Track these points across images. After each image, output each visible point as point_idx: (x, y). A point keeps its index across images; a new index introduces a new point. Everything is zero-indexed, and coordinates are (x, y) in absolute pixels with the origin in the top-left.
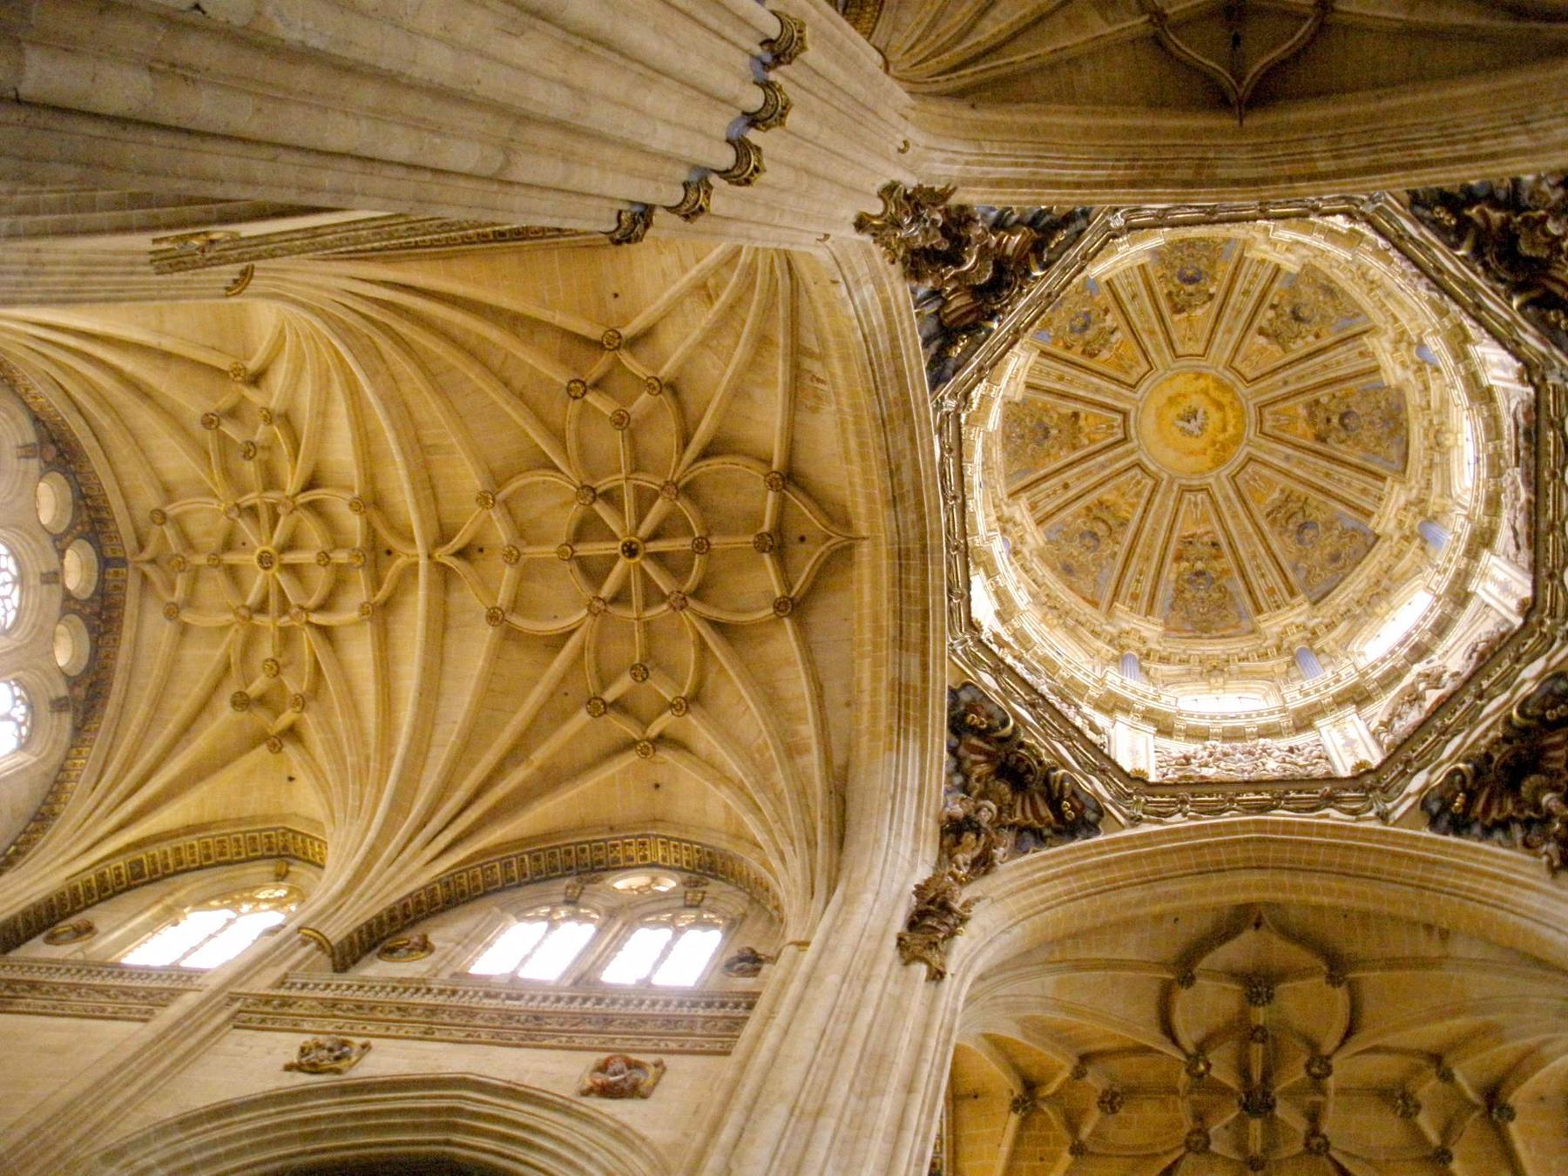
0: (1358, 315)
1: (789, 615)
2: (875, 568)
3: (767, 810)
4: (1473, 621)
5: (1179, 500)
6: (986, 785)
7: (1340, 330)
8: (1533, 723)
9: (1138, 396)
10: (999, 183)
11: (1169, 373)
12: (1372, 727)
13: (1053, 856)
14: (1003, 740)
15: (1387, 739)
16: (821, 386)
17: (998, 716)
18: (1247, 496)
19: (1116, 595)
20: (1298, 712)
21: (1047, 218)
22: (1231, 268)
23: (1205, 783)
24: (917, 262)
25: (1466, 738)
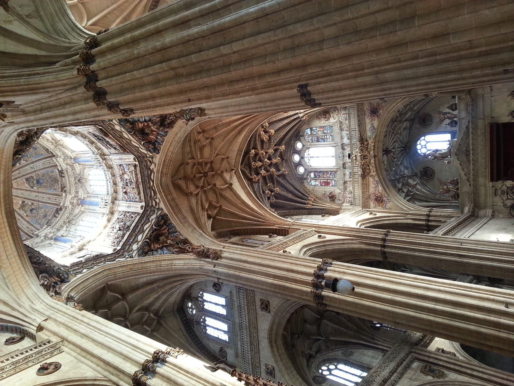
0: (40, 224)
10: (176, 134)
14: (32, 137)
22: (44, 191)
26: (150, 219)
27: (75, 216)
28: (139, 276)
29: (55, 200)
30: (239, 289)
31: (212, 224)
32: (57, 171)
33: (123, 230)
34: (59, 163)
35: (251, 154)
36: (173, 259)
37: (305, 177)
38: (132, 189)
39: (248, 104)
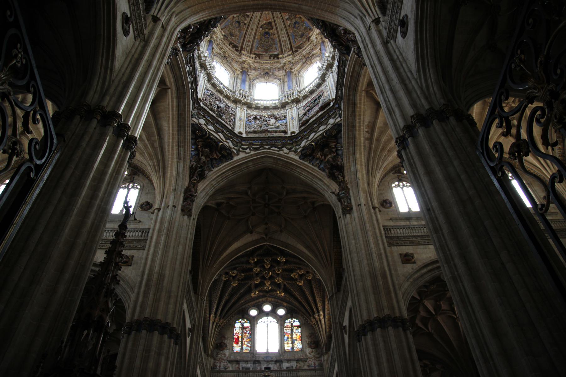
7: (228, 21)
10: (321, 180)
16: (366, 130)
21: (310, 158)
22: (256, 37)
24: (341, 169)
26: (228, 141)
27: (230, 63)
28: (171, 122)
29: (247, 47)
30: (146, 231)
31: (210, 207)
32: (276, 53)
33: (218, 111)
34: (286, 57)
35: (281, 258)
36: (184, 161)
37: (245, 316)
38: (260, 125)
39: (360, 262)
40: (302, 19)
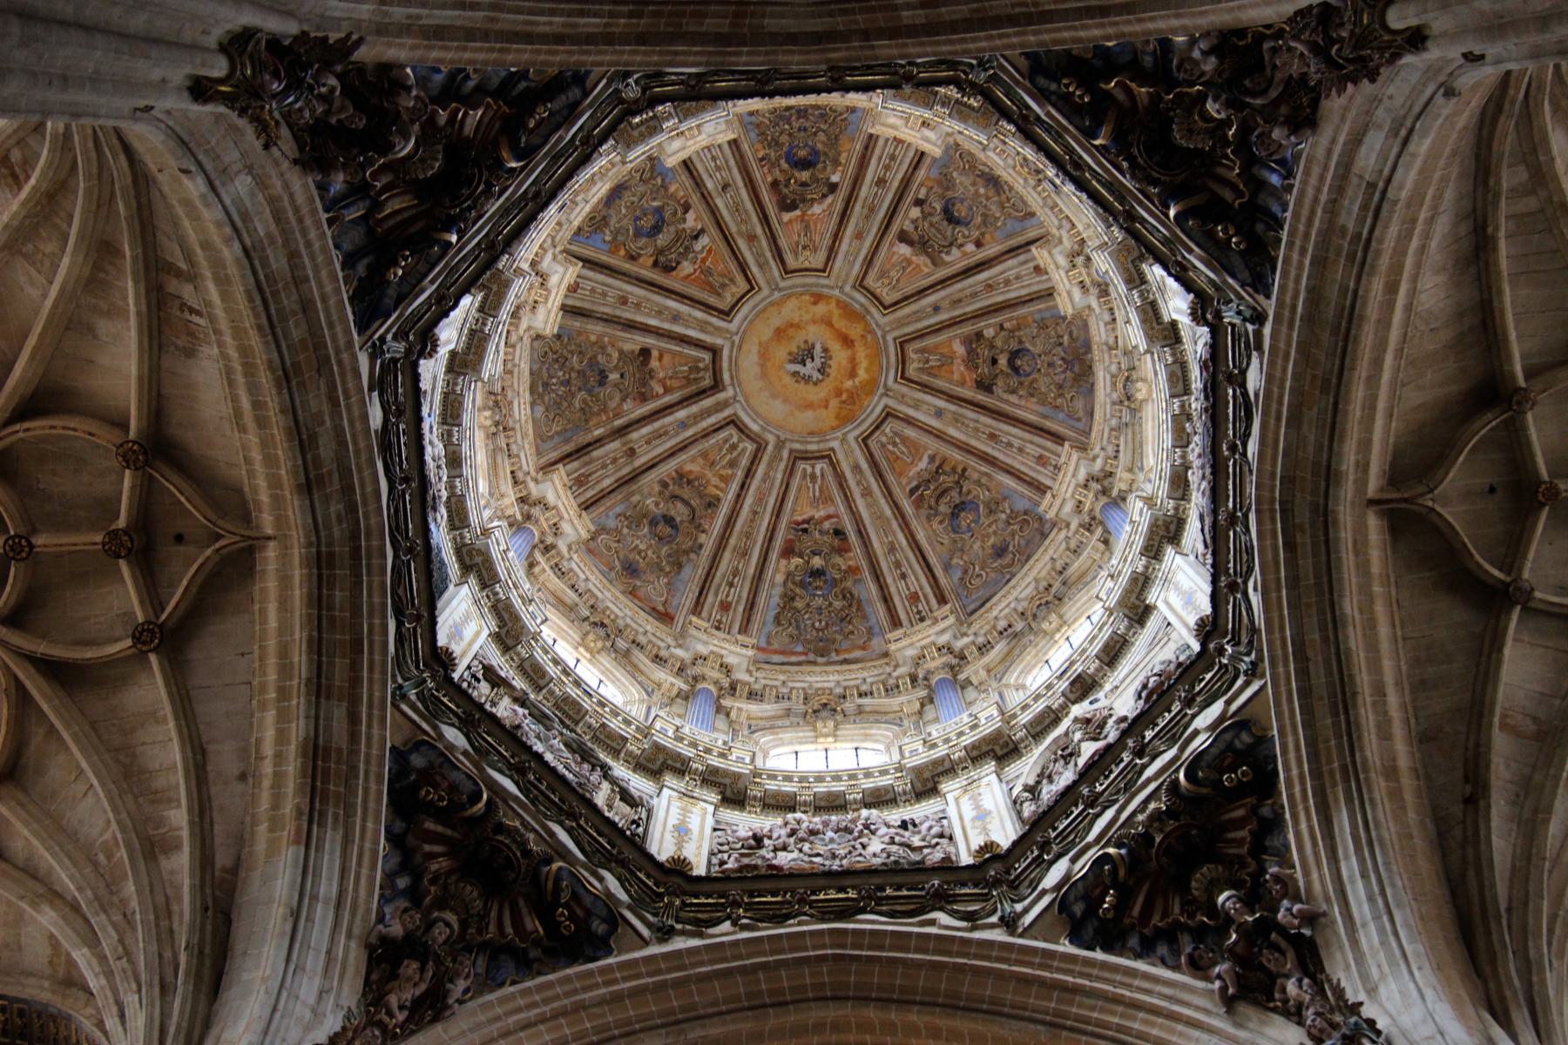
1: (154, 650)
2: (284, 580)
3: (108, 941)
4: (1152, 645)
5: (790, 472)
6: (445, 887)
7: (1010, 236)
8: (1204, 791)
9: (733, 326)
10: (439, 33)
11: (777, 295)
12: (1015, 792)
13: (540, 988)
15: (1028, 809)
17: (469, 786)
18: (884, 464)
19: (697, 608)
20: (918, 771)
21: (523, 85)
23: (776, 873)
25: (1119, 812)
36: (1346, 165)
40: (622, 252)
